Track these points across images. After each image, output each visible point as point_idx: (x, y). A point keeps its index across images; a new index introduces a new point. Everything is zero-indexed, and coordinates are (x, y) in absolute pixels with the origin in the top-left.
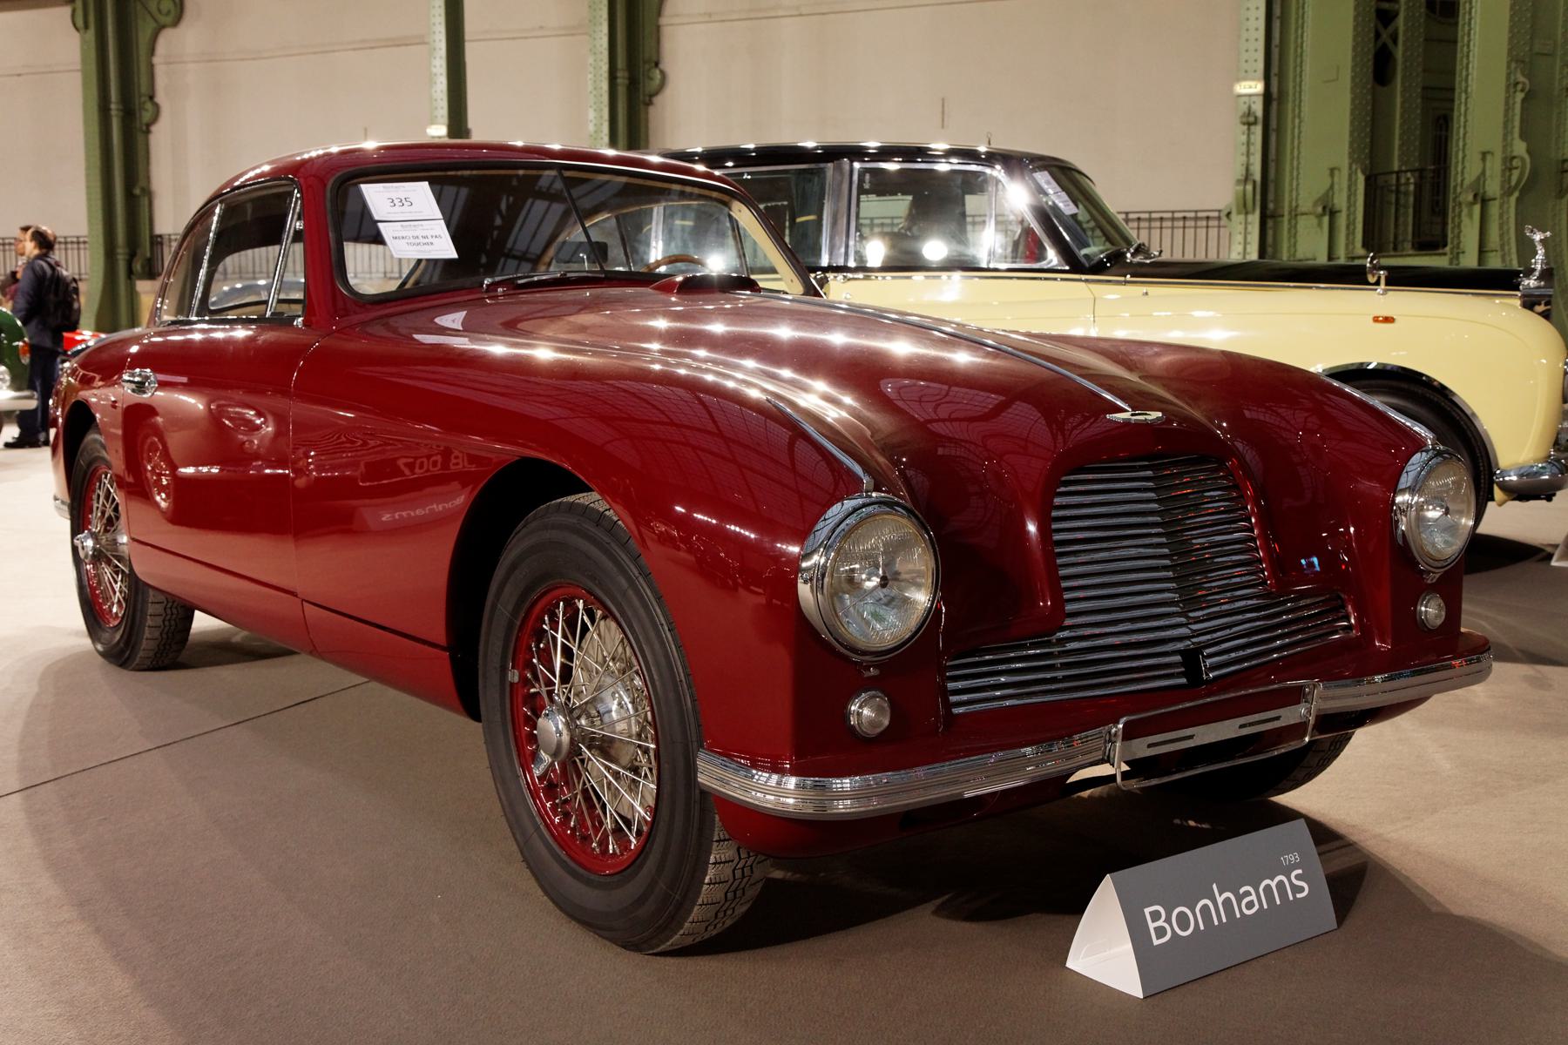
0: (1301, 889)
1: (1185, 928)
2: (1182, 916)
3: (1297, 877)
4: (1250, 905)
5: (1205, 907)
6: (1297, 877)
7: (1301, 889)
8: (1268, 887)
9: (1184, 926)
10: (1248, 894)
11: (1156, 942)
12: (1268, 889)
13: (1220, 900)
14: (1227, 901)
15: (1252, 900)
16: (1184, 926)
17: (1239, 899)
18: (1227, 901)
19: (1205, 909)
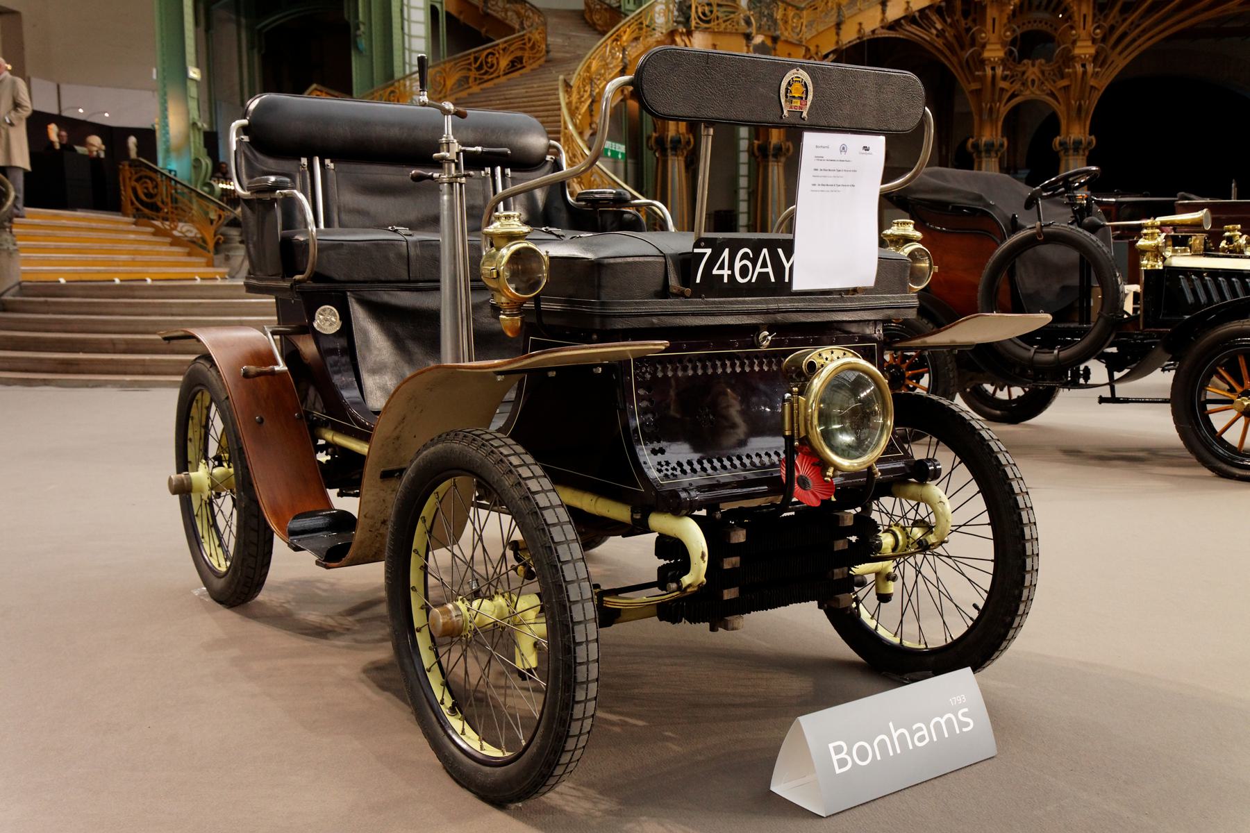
1: (863, 759)
3: (964, 715)
4: (921, 739)
5: (883, 740)
6: (964, 715)
7: (967, 724)
8: (938, 723)
9: (863, 758)
10: (920, 729)
11: (838, 771)
12: (938, 725)
13: (895, 735)
15: (923, 735)
16: (863, 758)
17: (912, 735)
19: (882, 742)
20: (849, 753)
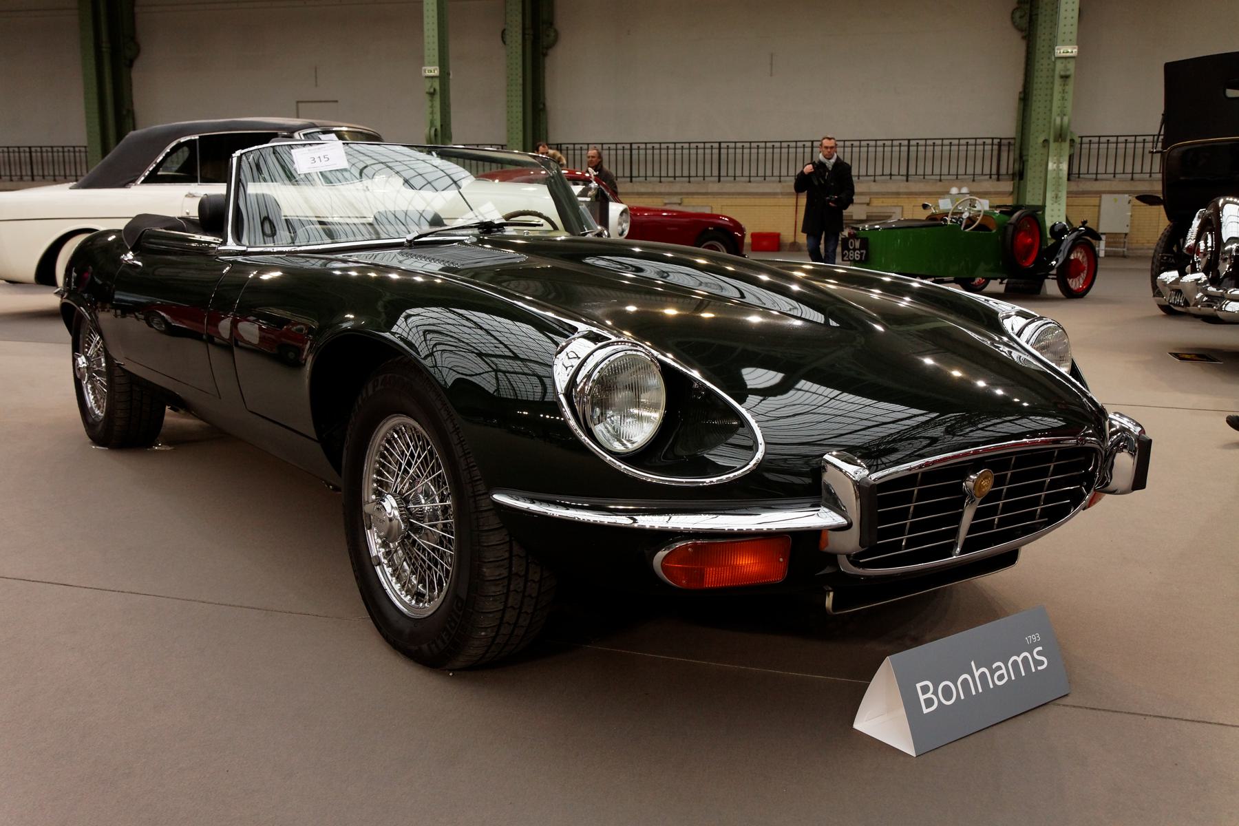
0: (1042, 663)
1: (948, 699)
2: (946, 689)
3: (1039, 653)
4: (1001, 677)
5: (965, 680)
6: (1039, 653)
7: (1042, 663)
8: (1015, 662)
9: (948, 697)
12: (1015, 663)
13: (977, 674)
14: (983, 674)
15: (1002, 674)
16: (948, 697)
17: (992, 672)
18: (983, 674)
19: (965, 681)
20: (935, 693)
